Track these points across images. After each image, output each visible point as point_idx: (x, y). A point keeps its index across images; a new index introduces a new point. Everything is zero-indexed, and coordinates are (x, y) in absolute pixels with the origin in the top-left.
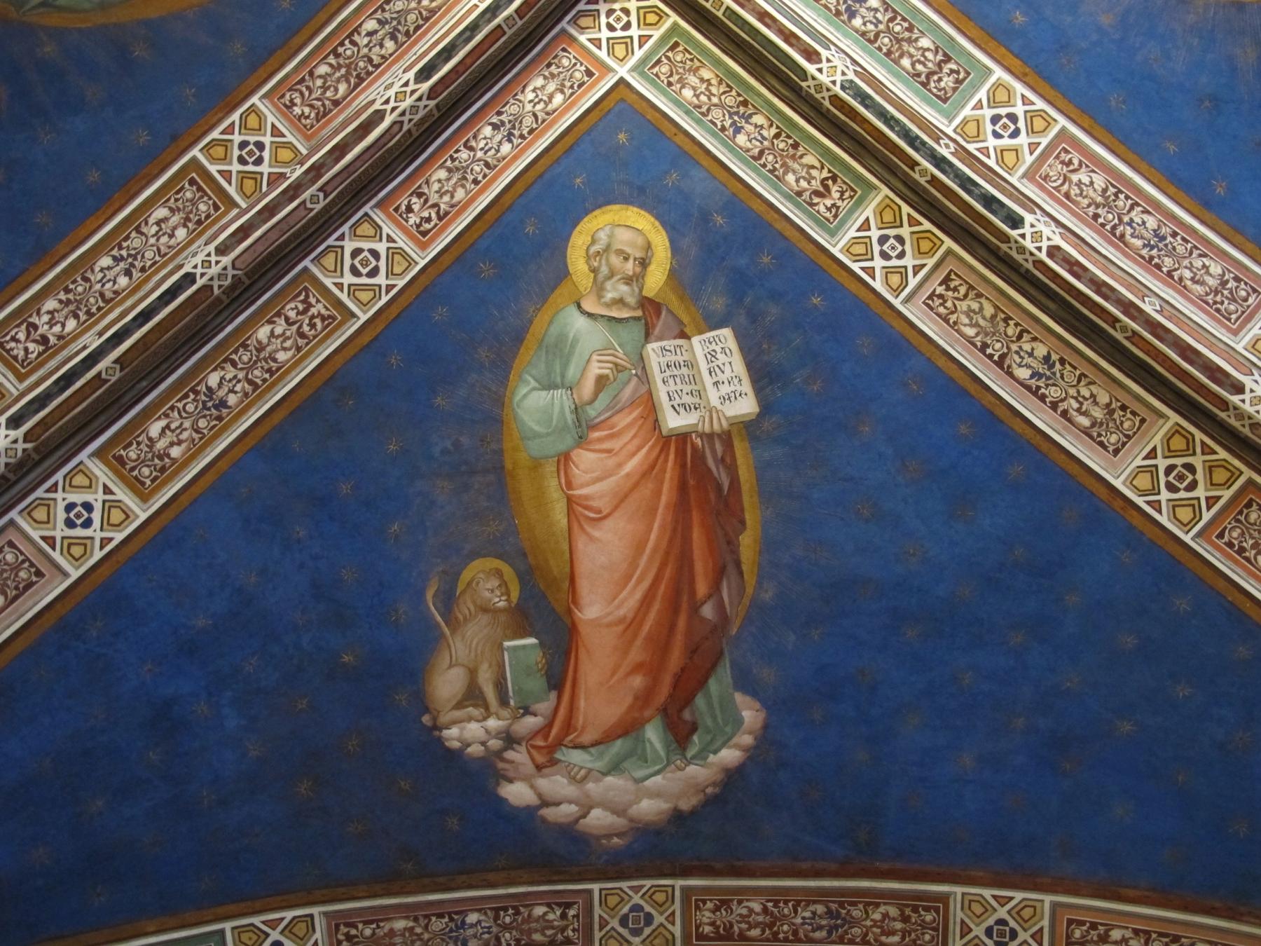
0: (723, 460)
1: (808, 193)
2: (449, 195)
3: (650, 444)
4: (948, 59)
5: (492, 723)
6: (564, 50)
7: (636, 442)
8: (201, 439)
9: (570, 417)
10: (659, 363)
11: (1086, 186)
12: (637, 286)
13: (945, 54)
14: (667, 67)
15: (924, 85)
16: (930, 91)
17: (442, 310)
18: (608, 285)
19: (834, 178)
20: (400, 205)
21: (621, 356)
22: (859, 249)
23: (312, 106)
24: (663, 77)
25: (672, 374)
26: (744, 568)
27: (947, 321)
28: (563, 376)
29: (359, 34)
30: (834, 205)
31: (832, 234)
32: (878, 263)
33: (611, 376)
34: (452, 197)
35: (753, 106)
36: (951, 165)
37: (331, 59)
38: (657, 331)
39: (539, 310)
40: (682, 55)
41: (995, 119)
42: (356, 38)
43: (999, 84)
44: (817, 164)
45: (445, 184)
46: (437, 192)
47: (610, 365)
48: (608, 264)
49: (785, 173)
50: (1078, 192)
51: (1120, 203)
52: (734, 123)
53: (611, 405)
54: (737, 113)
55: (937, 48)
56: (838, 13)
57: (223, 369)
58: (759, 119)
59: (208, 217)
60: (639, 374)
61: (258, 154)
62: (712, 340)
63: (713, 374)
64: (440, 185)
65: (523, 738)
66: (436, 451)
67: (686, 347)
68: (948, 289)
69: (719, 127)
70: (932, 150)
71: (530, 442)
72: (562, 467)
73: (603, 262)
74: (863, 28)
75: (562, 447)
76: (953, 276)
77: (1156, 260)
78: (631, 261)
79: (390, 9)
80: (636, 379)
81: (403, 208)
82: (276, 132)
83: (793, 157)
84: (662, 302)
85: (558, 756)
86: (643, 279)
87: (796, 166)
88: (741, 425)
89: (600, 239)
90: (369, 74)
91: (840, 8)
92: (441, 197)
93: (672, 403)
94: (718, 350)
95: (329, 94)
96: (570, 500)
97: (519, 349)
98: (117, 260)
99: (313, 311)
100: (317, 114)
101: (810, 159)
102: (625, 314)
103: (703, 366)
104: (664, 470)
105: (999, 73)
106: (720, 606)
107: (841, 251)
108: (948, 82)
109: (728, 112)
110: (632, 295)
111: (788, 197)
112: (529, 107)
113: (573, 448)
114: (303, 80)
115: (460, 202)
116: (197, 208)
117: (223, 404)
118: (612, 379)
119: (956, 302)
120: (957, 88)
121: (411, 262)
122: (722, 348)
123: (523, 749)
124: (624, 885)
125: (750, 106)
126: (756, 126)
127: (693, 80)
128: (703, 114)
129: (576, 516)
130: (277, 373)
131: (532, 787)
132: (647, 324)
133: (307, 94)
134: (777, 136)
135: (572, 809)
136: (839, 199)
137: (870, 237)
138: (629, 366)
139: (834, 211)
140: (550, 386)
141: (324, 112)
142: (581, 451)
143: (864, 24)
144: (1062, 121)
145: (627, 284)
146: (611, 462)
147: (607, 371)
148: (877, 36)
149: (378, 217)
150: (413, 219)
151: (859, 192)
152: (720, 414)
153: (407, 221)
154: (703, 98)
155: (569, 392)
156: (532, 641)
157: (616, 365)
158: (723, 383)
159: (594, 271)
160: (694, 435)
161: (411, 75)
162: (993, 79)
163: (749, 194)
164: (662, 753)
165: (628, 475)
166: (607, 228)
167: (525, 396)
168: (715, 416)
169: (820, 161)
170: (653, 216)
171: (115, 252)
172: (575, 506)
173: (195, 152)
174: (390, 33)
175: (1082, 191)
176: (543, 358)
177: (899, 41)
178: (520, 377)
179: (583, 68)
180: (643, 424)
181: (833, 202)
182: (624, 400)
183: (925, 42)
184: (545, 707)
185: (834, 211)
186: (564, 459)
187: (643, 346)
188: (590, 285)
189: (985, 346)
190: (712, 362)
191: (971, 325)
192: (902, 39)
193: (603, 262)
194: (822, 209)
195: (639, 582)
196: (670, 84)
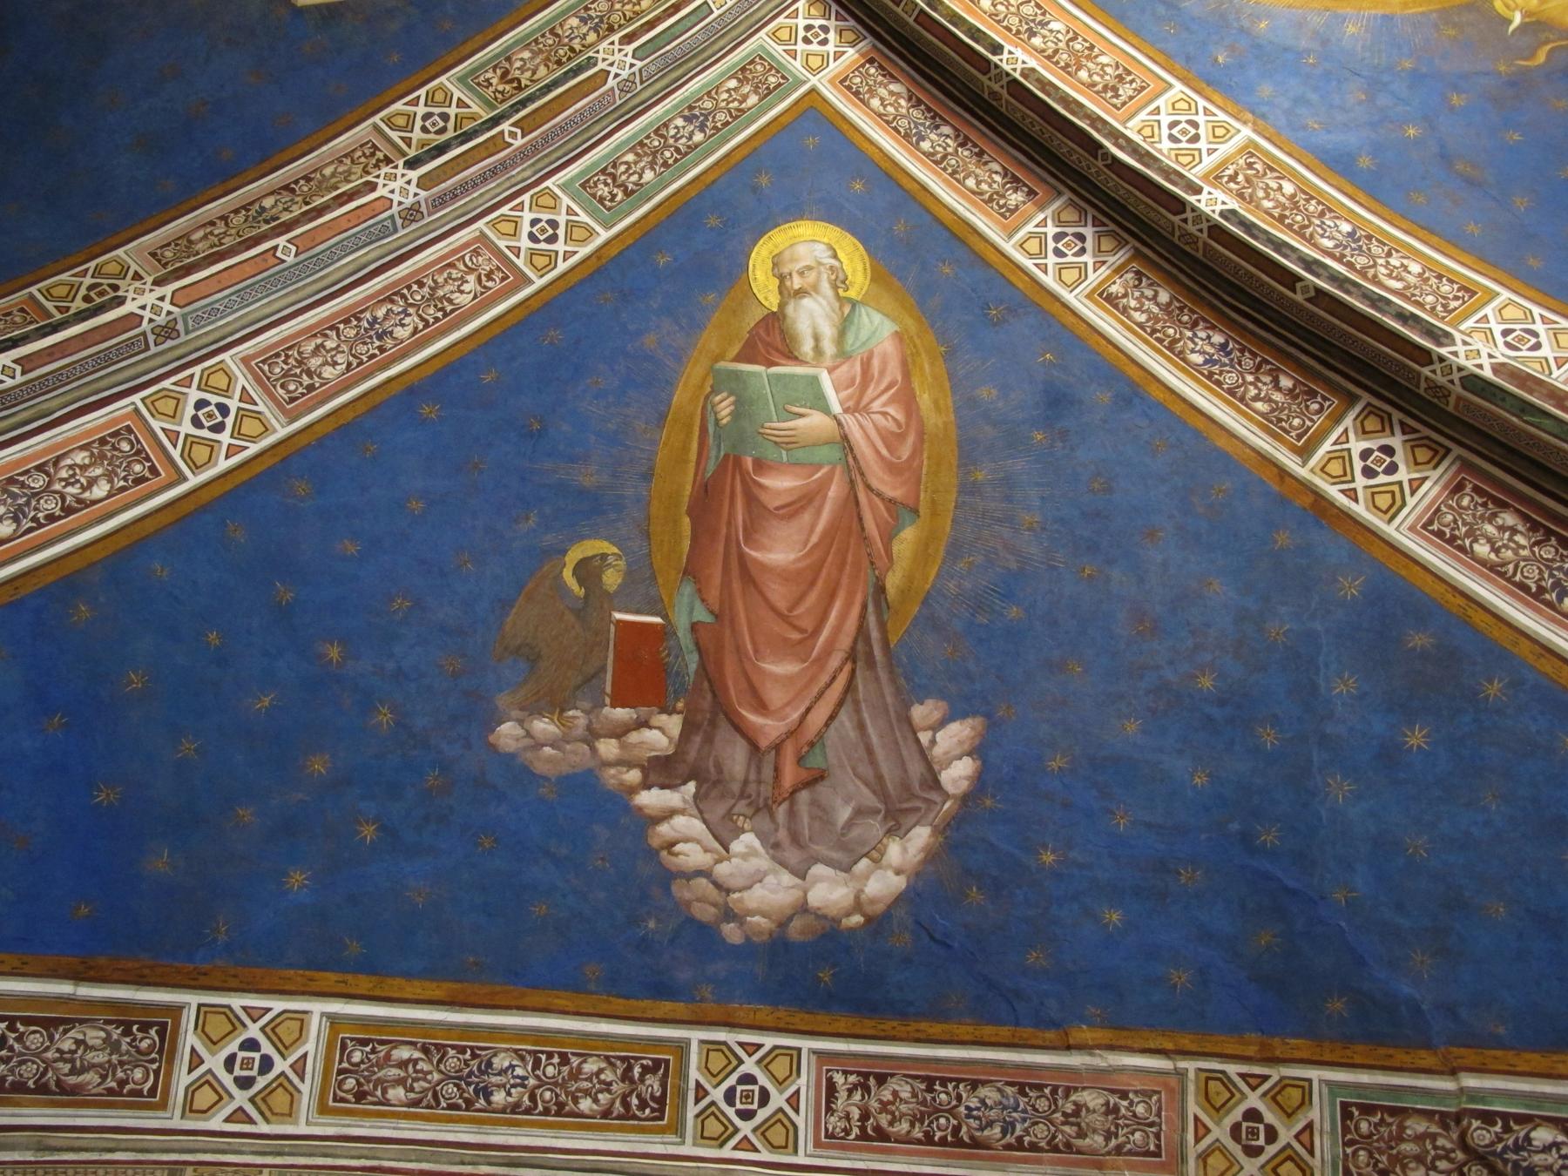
4: (628, 193)
11: (459, 286)
13: (633, 192)
15: (603, 171)
16: (597, 174)
36: (489, 129)
44: (535, 77)
49: (532, 51)
50: (454, 276)
52: (591, 18)
54: (602, 21)
55: (642, 185)
56: (691, 108)
70: (508, 118)
83: (548, 59)
108: (603, 191)
126: (585, 35)
143: (676, 127)
148: (662, 136)
162: (598, 228)
175: (454, 280)
177: (654, 154)
183: (648, 176)
192: (655, 157)
194: (489, 75)
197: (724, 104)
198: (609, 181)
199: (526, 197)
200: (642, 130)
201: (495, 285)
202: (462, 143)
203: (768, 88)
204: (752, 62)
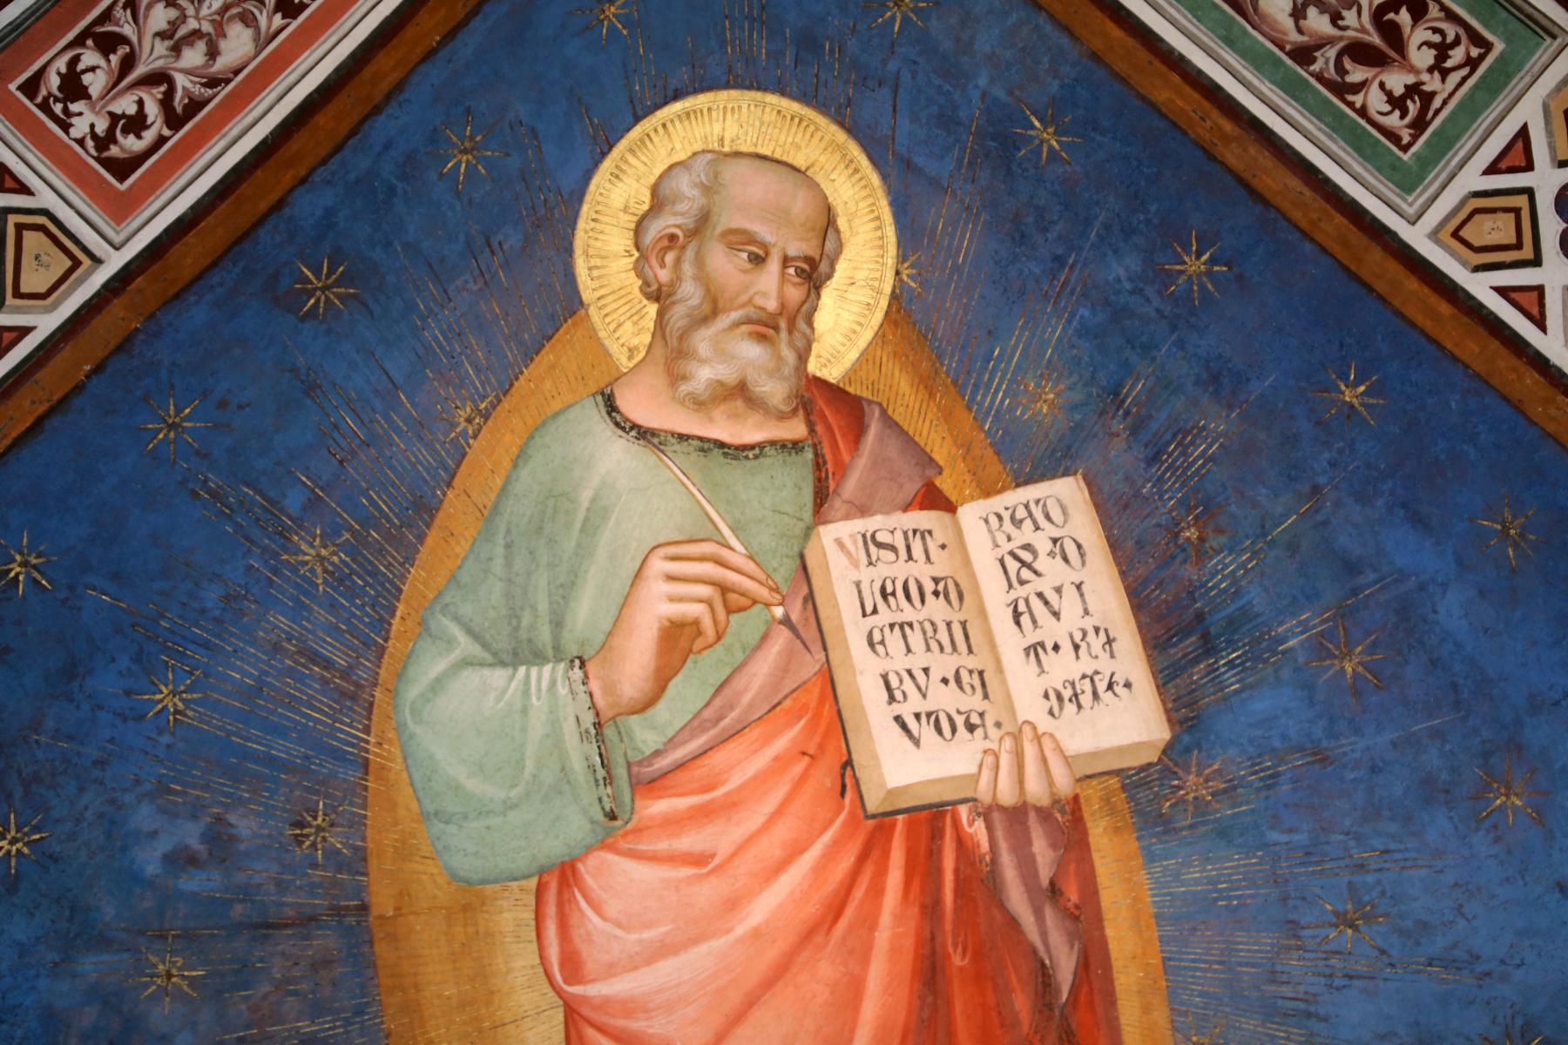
0: (1054, 890)
1: (1332, 53)
2: (201, 46)
3: (827, 837)
7: (784, 831)
9: (579, 754)
10: (858, 584)
12: (791, 344)
17: (178, 411)
18: (702, 341)
20: (42, 72)
21: (739, 560)
22: (1496, 230)
25: (900, 618)
28: (558, 624)
30: (1413, 90)
31: (1407, 180)
34: (213, 53)
38: (851, 485)
39: (486, 417)
45: (191, 11)
46: (162, 35)
47: (704, 591)
48: (702, 277)
53: (707, 714)
60: (794, 617)
62: (1021, 513)
63: (1025, 619)
64: (173, 13)
66: (150, 860)
67: (939, 537)
71: (452, 829)
72: (551, 910)
73: (688, 268)
75: (553, 848)
78: (774, 266)
80: (782, 636)
81: (54, 81)
84: (866, 394)
86: (810, 323)
88: (1114, 782)
89: (677, 197)
92: (176, 50)
93: (897, 709)
94: (1043, 544)
96: (573, 1014)
97: (421, 538)
102: (751, 432)
103: (995, 594)
104: (869, 922)
107: (1434, 235)
110: (775, 372)
113: (589, 850)
115: (237, 72)
118: (710, 632)
121: (78, 258)
122: (1055, 541)
132: (819, 464)
136: (1430, 70)
137: (1529, 192)
138: (763, 593)
139: (1413, 108)
142: (611, 857)
145: (761, 338)
146: (707, 893)
151: (1499, 46)
152: (1048, 745)
153: (66, 127)
155: (577, 673)
157: (724, 589)
158: (1056, 648)
159: (659, 295)
160: (964, 812)
163: (1143, 54)
165: (756, 933)
166: (702, 161)
167: (438, 685)
168: (1030, 751)
170: (841, 124)
172: (590, 1032)
176: (498, 566)
178: (422, 623)
180: (804, 777)
181: (1411, 79)
182: (746, 699)
185: (1413, 108)
187: (808, 533)
188: (647, 338)
190: (1022, 582)
193: (688, 268)
194: (1376, 101)
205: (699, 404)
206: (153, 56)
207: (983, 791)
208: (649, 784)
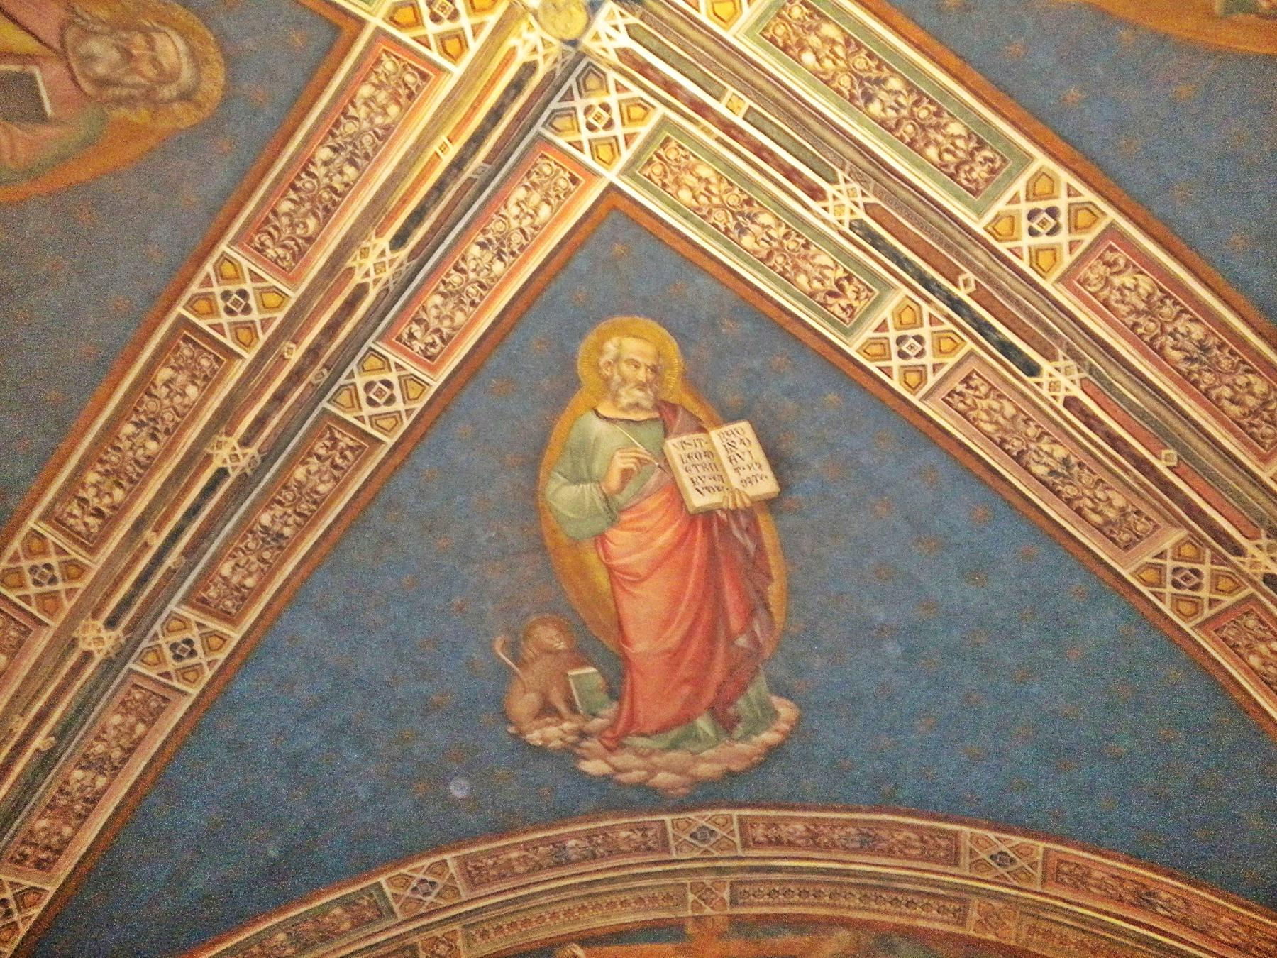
0: (747, 530)
1: (823, 294)
4: (981, 145)
5: (567, 726)
6: (543, 156)
8: (269, 567)
9: (600, 505)
14: (660, 167)
18: (622, 392)
19: (849, 278)
22: (876, 349)
23: (284, 247)
24: (656, 179)
26: (773, 610)
27: (964, 415)
29: (313, 164)
31: (847, 333)
32: (896, 362)
33: (635, 469)
35: (758, 203)
36: (968, 307)
37: (292, 195)
38: (675, 429)
40: (675, 152)
41: (1032, 215)
42: (312, 169)
43: (1040, 174)
44: (831, 264)
47: (634, 460)
48: (620, 373)
50: (1119, 297)
51: (1166, 310)
56: (852, 98)
57: (272, 509)
58: (765, 219)
59: (214, 372)
61: (244, 303)
65: (595, 734)
68: (969, 387)
69: (723, 230)
74: (883, 115)
76: (975, 376)
77: (1196, 376)
79: (341, 135)
80: (659, 471)
81: (405, 336)
82: (256, 278)
83: (805, 258)
85: (626, 742)
87: (808, 267)
90: (335, 204)
91: (854, 91)
92: (441, 321)
94: (736, 440)
95: (299, 231)
98: (139, 425)
99: (341, 444)
100: (293, 255)
101: (824, 259)
102: (641, 416)
105: (1042, 161)
106: (755, 641)
108: (980, 172)
109: (732, 213)
111: (798, 298)
112: (515, 224)
114: (267, 221)
116: (199, 364)
117: (280, 536)
119: (977, 400)
120: (991, 179)
123: (595, 740)
124: (691, 815)
125: (755, 205)
126: (763, 226)
127: (689, 179)
128: (703, 217)
129: (618, 581)
130: (322, 504)
131: (607, 762)
132: (665, 424)
133: (275, 233)
134: (786, 236)
135: (644, 773)
140: (579, 480)
141: (300, 250)
144: (1112, 214)
145: (641, 390)
146: (644, 538)
147: (632, 465)
148: (898, 124)
149: (382, 348)
150: (417, 346)
154: (703, 199)
156: (592, 670)
161: (384, 242)
162: (1033, 168)
164: (711, 733)
167: (557, 490)
168: (737, 496)
169: (834, 261)
171: (134, 418)
173: (180, 310)
174: (347, 159)
177: (923, 127)
179: (567, 175)
184: (609, 711)
185: (849, 311)
186: (600, 539)
187: (663, 443)
189: (1004, 441)
191: (991, 422)
193: (615, 371)
195: (680, 623)
196: (664, 185)
197: (841, 63)
198: (967, 168)
199: (1002, 247)
200: (891, 144)
201: (1121, 257)
202: (994, 330)
203: (811, 16)
204: (773, 40)
205: (624, 410)
206: (434, 324)
207: (724, 506)
208: (622, 511)
